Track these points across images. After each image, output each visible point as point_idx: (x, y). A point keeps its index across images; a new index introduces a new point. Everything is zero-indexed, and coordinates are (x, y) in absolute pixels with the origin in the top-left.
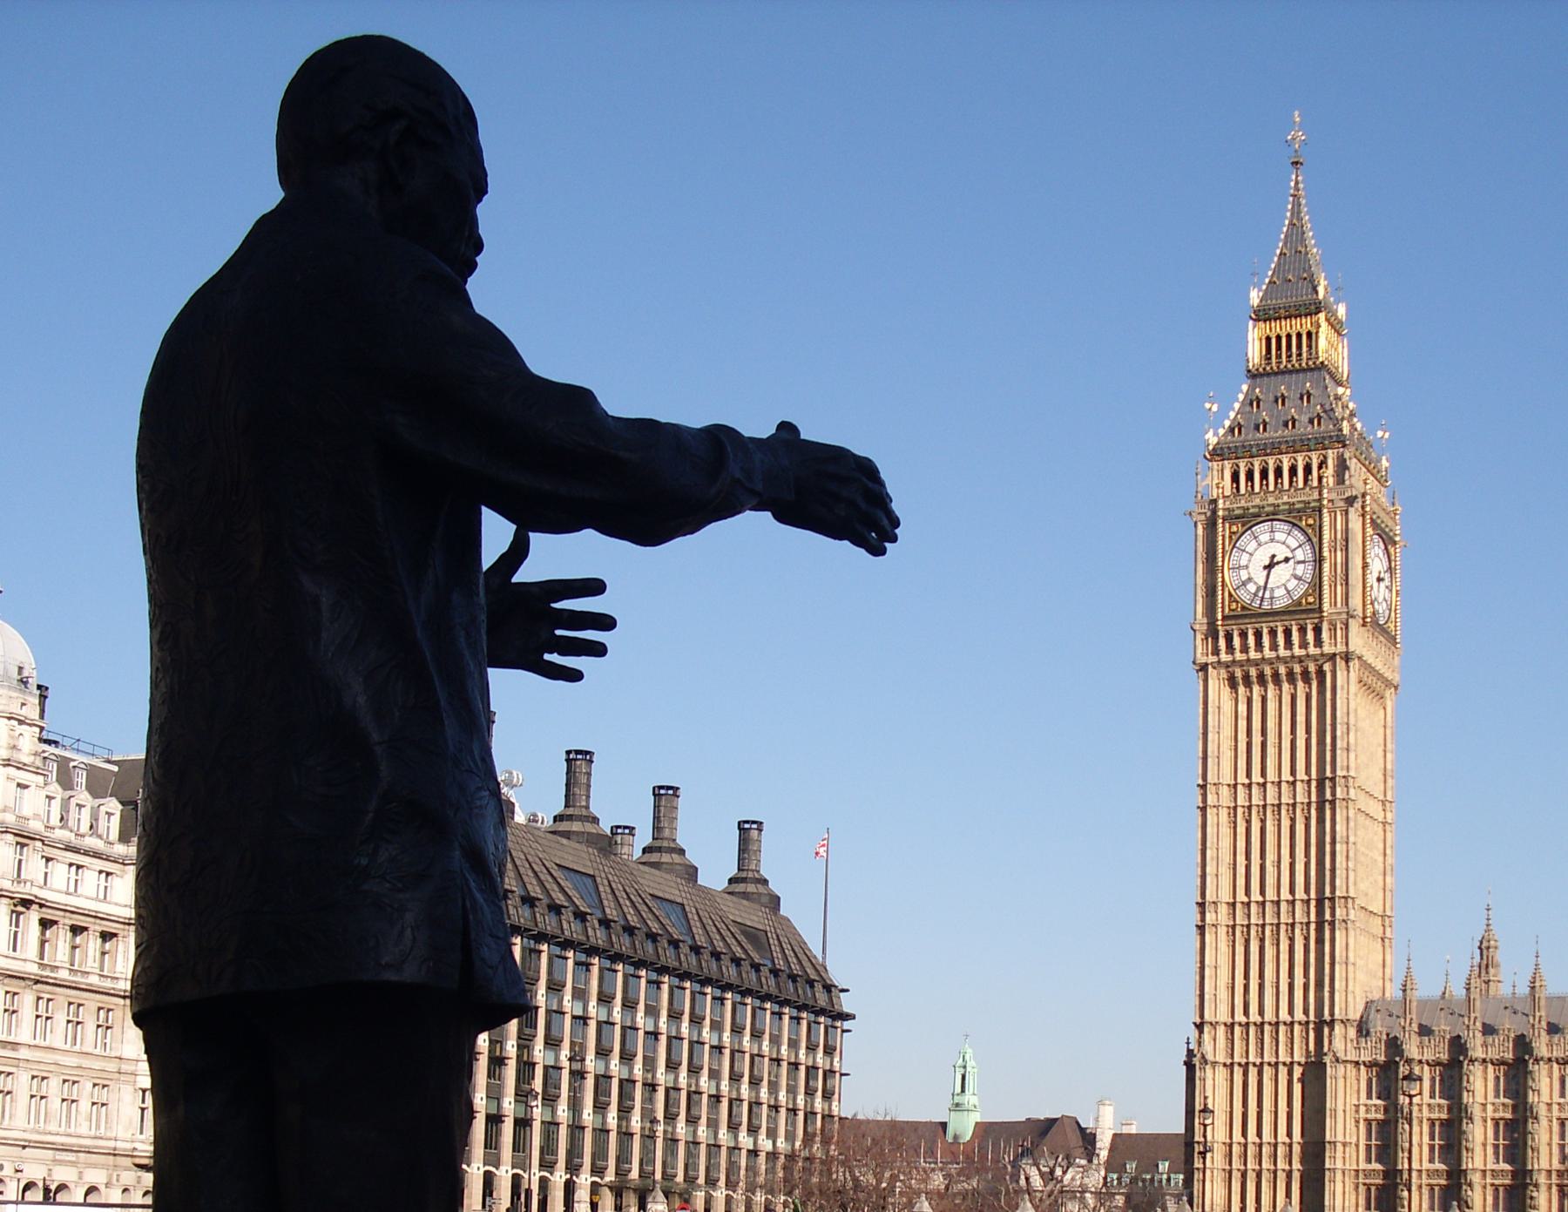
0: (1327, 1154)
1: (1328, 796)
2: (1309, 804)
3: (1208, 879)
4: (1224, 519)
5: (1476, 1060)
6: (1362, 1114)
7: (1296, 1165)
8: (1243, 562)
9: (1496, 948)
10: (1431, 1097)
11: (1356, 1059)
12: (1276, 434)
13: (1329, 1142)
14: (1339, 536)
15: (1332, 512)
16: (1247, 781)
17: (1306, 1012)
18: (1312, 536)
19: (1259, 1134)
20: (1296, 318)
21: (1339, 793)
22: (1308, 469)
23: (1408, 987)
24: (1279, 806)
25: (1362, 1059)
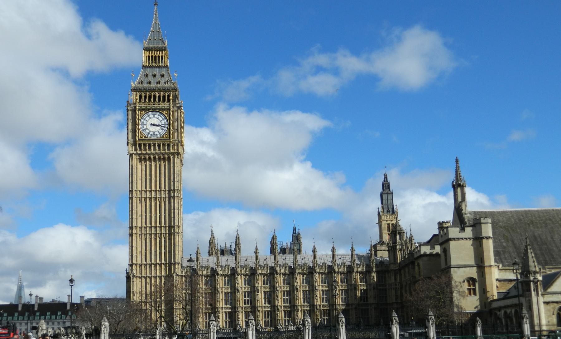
1: (172, 195)
2: (166, 197)
3: (134, 219)
4: (138, 109)
7: (163, 307)
8: (145, 123)
11: (182, 275)
12: (154, 85)
14: (175, 118)
15: (173, 110)
17: (165, 260)
18: (167, 117)
20: (158, 51)
22: (164, 97)
24: (156, 198)
25: (184, 274)
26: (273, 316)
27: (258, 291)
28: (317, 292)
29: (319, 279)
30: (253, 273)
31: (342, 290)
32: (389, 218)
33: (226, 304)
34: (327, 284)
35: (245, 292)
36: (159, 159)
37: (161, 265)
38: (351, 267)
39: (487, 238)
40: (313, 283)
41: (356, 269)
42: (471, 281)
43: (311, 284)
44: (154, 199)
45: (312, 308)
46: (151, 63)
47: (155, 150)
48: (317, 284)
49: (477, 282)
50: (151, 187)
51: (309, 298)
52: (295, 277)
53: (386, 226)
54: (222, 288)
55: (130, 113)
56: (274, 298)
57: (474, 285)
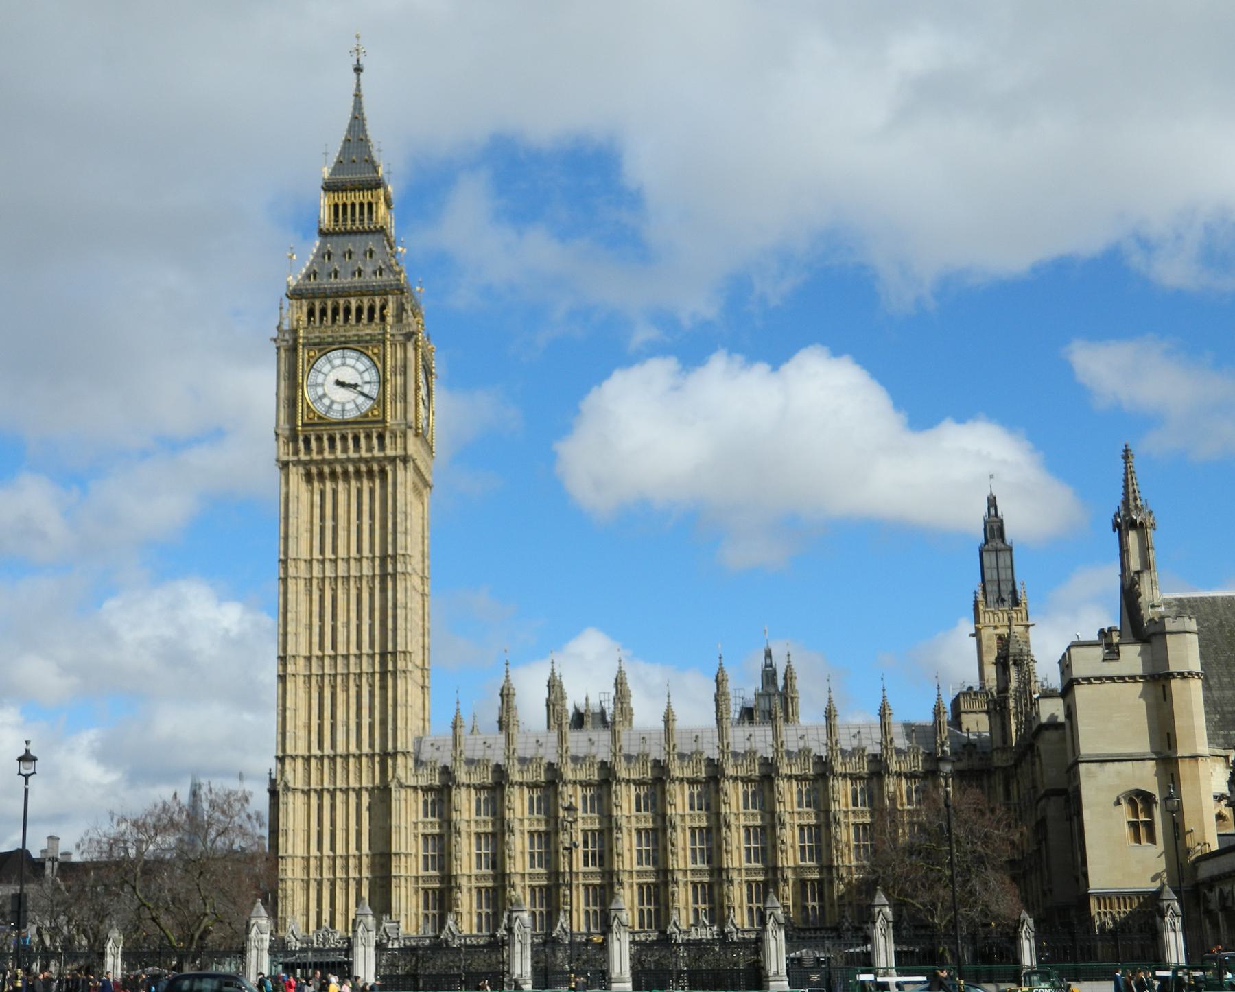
0: (393, 864)
1: (390, 569)
2: (373, 576)
3: (289, 637)
4: (304, 346)
5: (516, 783)
6: (420, 830)
7: (366, 873)
9: (514, 694)
10: (477, 815)
11: (415, 784)
12: (345, 281)
13: (395, 854)
14: (399, 363)
15: (393, 345)
16: (320, 557)
17: (372, 745)
19: (333, 848)
20: (359, 191)
21: (400, 568)
22: (372, 310)
23: (458, 724)
24: (348, 578)
25: (420, 783)
26: (662, 901)
27: (619, 829)
28: (784, 830)
29: (792, 794)
30: (659, 778)
31: (856, 825)
32: (1001, 619)
33: (532, 866)
34: (814, 807)
35: (585, 832)
36: (358, 473)
37: (359, 757)
38: (880, 761)
39: (1183, 676)
40: (773, 806)
41: (894, 767)
42: (1139, 799)
43: (768, 809)
44: (343, 582)
45: (770, 876)
46: (357, 222)
47: (345, 450)
48: (783, 809)
49: (1156, 803)
50: (334, 550)
51: (707, 849)
52: (722, 788)
53: (994, 643)
54: (630, 817)
55: (283, 354)
56: (665, 849)
57: (1150, 813)
